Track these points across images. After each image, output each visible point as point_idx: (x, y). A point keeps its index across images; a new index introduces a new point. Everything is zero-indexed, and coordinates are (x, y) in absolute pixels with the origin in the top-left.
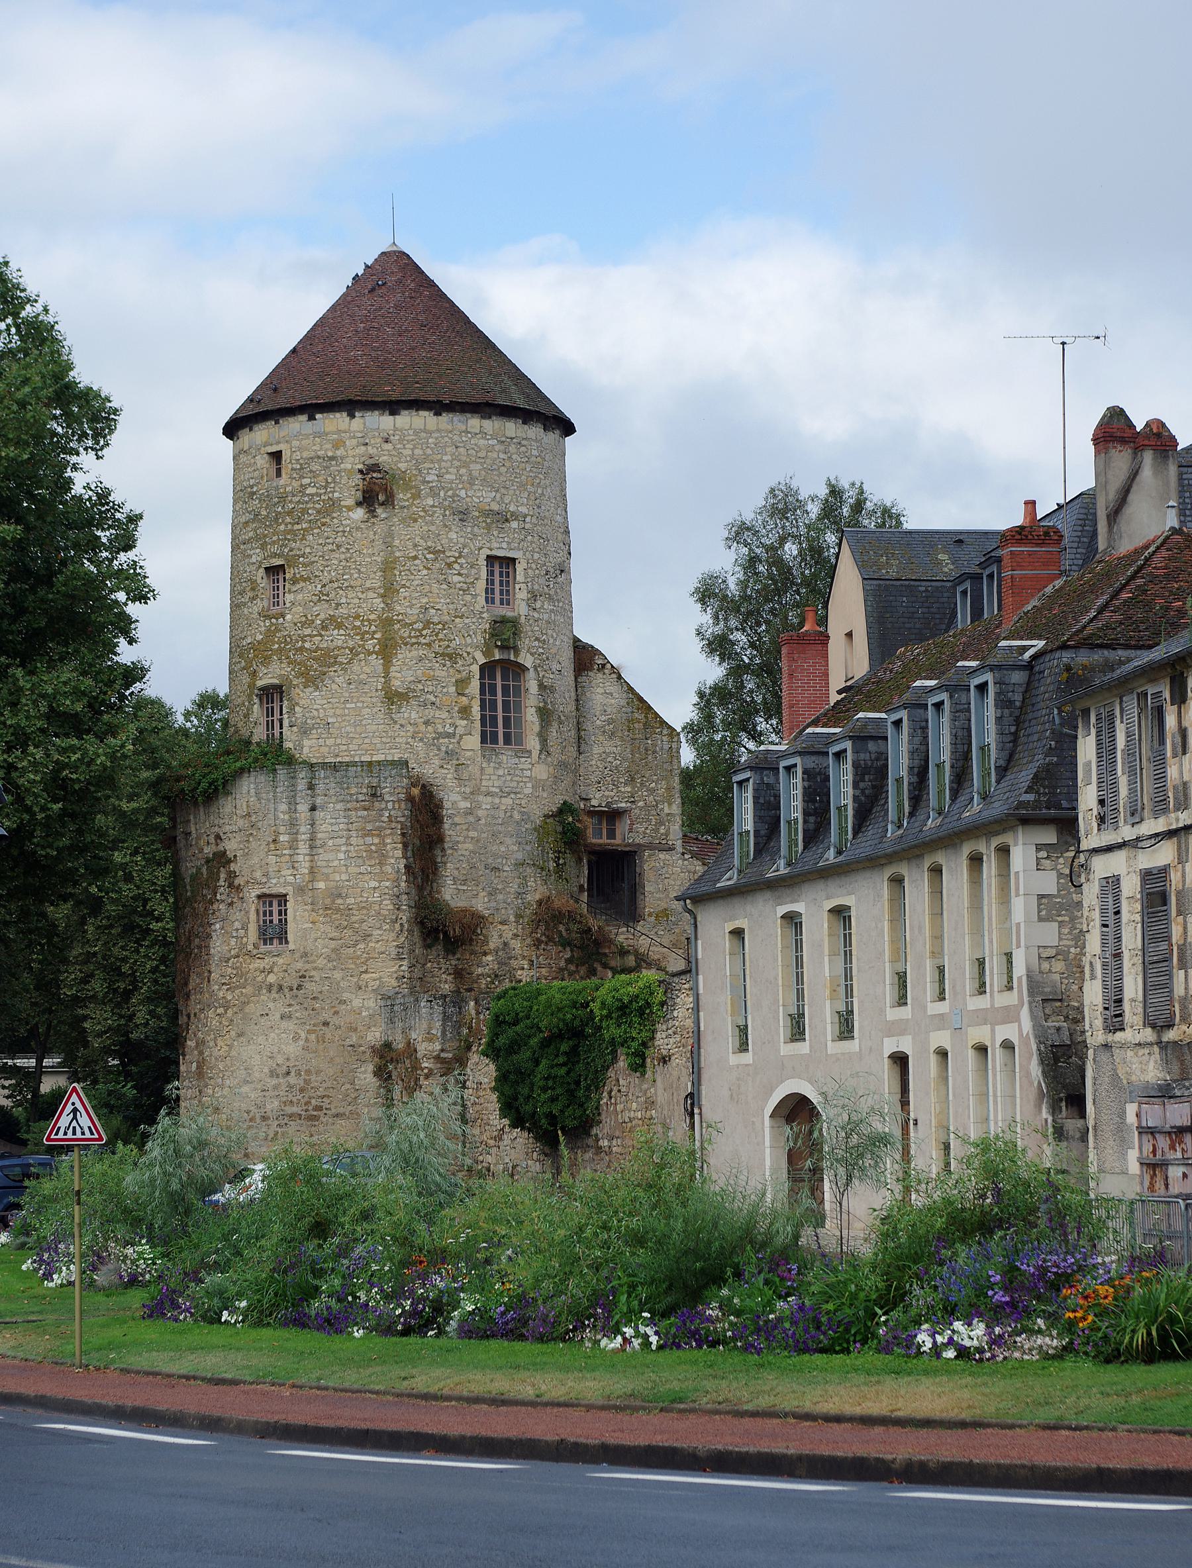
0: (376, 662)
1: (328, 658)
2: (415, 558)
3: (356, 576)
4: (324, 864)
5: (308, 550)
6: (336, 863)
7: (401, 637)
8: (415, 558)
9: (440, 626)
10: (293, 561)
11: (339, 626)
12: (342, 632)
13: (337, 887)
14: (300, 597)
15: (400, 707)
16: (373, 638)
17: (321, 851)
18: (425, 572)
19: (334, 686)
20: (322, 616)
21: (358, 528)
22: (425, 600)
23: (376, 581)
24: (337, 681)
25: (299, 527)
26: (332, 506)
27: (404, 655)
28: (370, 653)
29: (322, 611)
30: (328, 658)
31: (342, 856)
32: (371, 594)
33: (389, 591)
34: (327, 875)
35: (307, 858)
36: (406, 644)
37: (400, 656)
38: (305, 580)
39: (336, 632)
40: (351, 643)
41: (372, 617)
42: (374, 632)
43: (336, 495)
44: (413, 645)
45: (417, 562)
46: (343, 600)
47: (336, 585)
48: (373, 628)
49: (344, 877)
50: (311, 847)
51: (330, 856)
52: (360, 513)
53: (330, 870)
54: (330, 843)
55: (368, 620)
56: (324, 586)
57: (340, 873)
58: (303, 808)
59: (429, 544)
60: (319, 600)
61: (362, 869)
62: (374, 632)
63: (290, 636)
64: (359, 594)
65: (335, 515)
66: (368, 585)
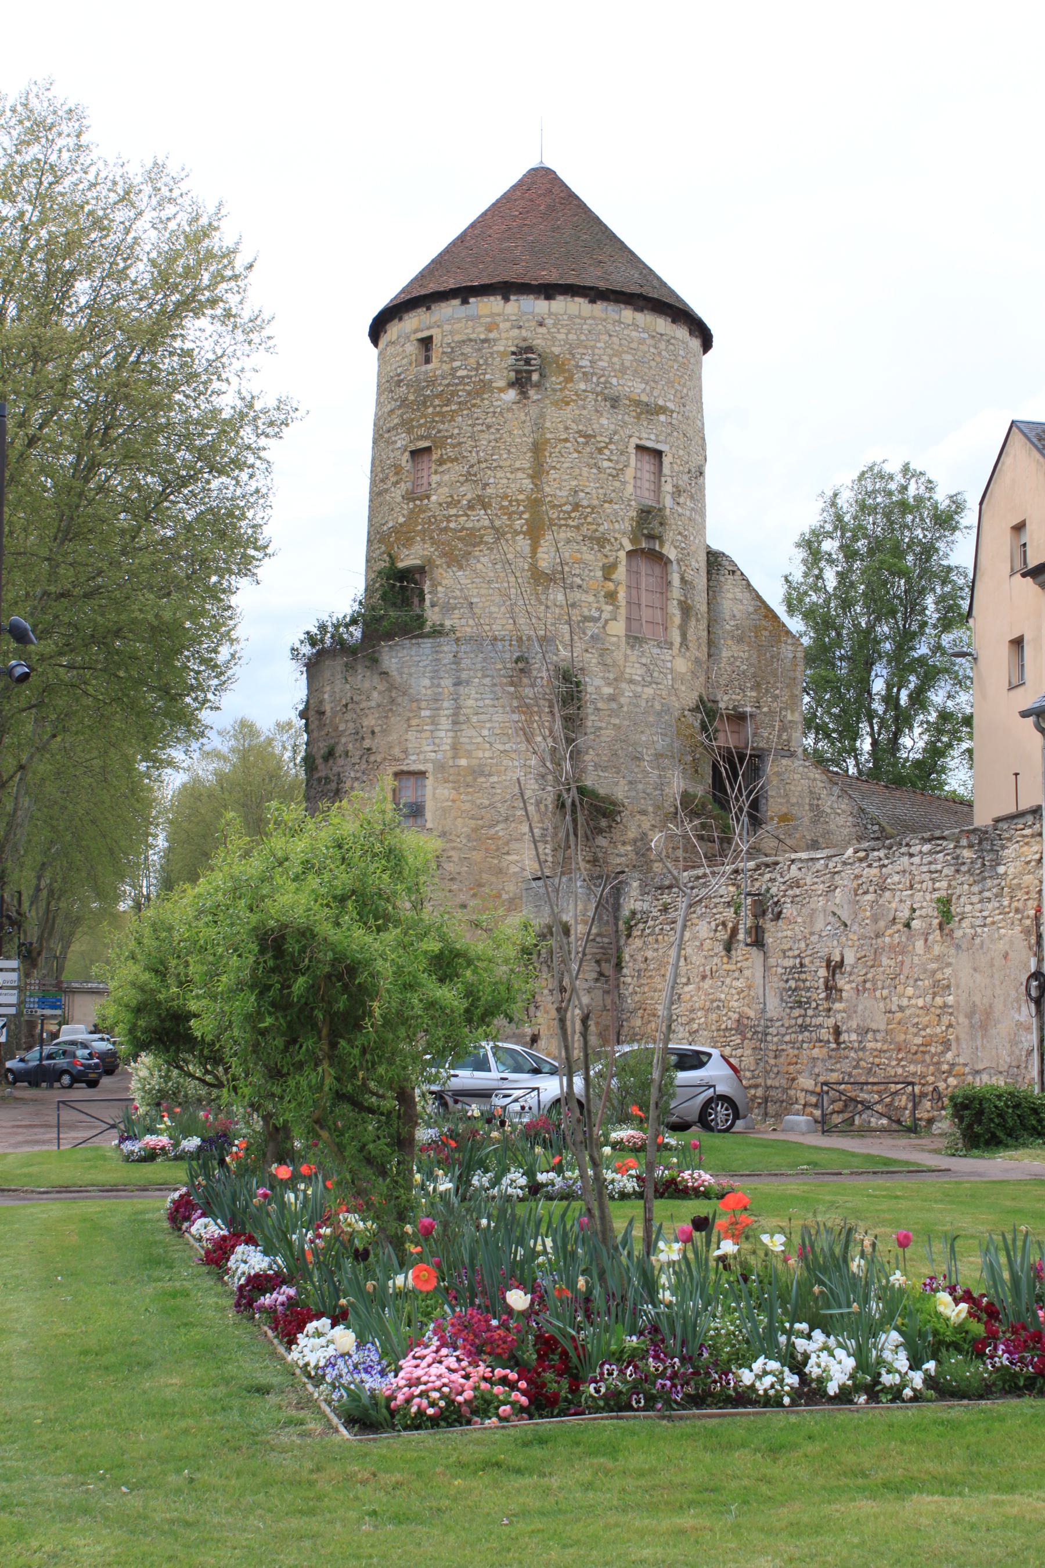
0: (523, 544)
1: (473, 538)
2: (566, 440)
4: (466, 740)
5: (456, 431)
8: (566, 440)
10: (440, 442)
13: (480, 765)
14: (446, 478)
16: (521, 518)
17: (464, 727)
18: (576, 455)
19: (479, 566)
20: (469, 496)
21: (509, 410)
22: (574, 483)
23: (525, 461)
24: (483, 561)
26: (485, 387)
28: (517, 533)
29: (468, 492)
30: (473, 538)
32: (520, 475)
33: (538, 473)
34: (469, 752)
35: (450, 734)
38: (452, 461)
41: (521, 497)
42: (523, 513)
43: (488, 377)
44: (560, 526)
45: (568, 445)
46: (492, 481)
47: (483, 465)
48: (521, 508)
49: (487, 754)
50: (455, 723)
51: (472, 732)
52: (512, 394)
53: (473, 747)
54: (474, 719)
55: (517, 500)
56: (472, 466)
57: (484, 750)
58: (447, 682)
60: (467, 480)
61: (507, 747)
62: (523, 513)
63: (434, 517)
64: (509, 475)
65: (485, 396)
66: (518, 465)
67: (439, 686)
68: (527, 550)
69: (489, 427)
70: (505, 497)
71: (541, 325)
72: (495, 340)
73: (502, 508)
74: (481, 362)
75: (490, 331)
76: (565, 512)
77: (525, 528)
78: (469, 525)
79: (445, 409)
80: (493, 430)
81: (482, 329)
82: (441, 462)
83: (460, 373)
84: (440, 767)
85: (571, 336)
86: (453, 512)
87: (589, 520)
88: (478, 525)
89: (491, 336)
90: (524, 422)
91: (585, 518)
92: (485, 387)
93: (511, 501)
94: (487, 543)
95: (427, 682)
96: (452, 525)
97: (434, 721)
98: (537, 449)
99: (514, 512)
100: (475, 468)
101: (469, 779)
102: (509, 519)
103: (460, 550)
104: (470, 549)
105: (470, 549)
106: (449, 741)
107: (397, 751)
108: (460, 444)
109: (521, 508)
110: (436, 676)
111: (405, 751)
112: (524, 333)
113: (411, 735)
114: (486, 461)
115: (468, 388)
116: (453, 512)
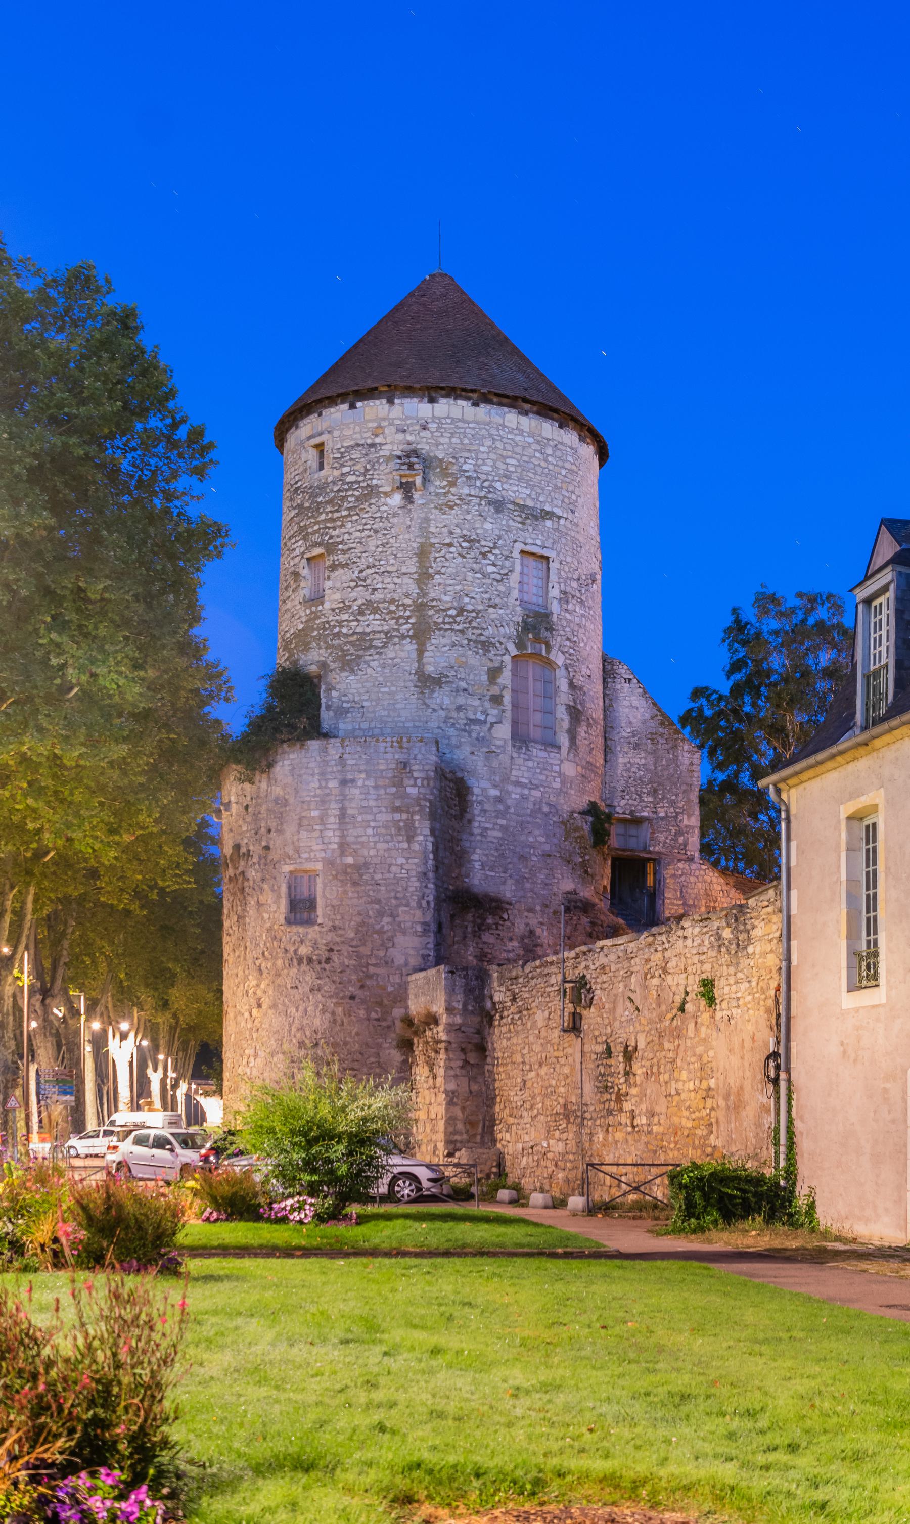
0: (410, 647)
1: (363, 642)
2: (450, 545)
3: (392, 561)
6: (364, 839)
7: (436, 623)
8: (450, 545)
9: (474, 614)
11: (375, 611)
12: (378, 616)
15: (433, 691)
16: (407, 623)
20: (359, 602)
21: (395, 515)
23: (411, 566)
25: (338, 515)
26: (371, 492)
28: (403, 637)
29: (360, 596)
31: (370, 831)
36: (440, 629)
37: (433, 641)
39: (372, 617)
40: (386, 628)
42: (409, 617)
43: (374, 482)
44: (446, 630)
45: (453, 549)
47: (373, 570)
51: (360, 831)
56: (361, 571)
58: (333, 784)
59: (465, 532)
62: (409, 617)
66: (404, 570)
67: (326, 787)
68: (414, 655)
69: (376, 531)
70: (392, 601)
71: (424, 428)
72: (381, 444)
73: (390, 612)
74: (368, 467)
75: (377, 436)
76: (450, 616)
77: (411, 633)
78: (359, 630)
79: (336, 515)
80: (380, 535)
81: (369, 434)
82: (333, 567)
83: (350, 479)
85: (453, 440)
86: (345, 617)
87: (474, 624)
88: (368, 630)
89: (378, 440)
90: (409, 527)
91: (470, 622)
92: (371, 492)
93: (398, 606)
94: (376, 647)
96: (344, 630)
97: (322, 819)
99: (401, 617)
100: (364, 574)
101: (356, 877)
102: (397, 623)
103: (352, 654)
104: (361, 652)
105: (361, 652)
106: (337, 839)
108: (350, 549)
109: (408, 613)
112: (410, 438)
113: (304, 834)
114: (374, 566)
115: (356, 493)
116: (345, 617)
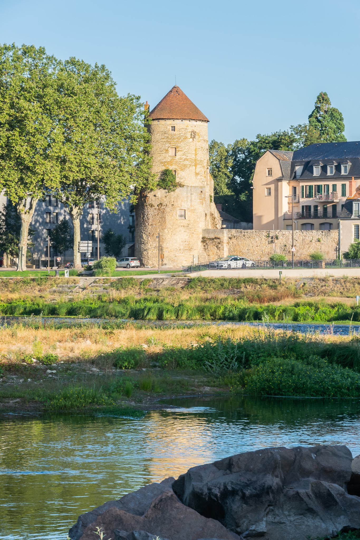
0: (194, 167)
1: (185, 166)
11: (187, 160)
26: (186, 138)
27: (198, 166)
52: (191, 140)
58: (189, 194)
84: (188, 209)
92: (186, 138)
95: (185, 194)
97: (187, 200)
98: (196, 150)
107: (179, 205)
110: (187, 192)
111: (181, 206)
113: (183, 203)
